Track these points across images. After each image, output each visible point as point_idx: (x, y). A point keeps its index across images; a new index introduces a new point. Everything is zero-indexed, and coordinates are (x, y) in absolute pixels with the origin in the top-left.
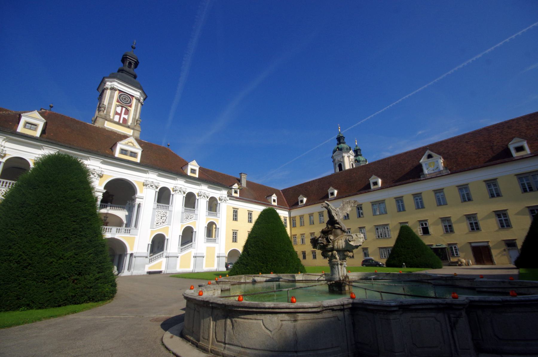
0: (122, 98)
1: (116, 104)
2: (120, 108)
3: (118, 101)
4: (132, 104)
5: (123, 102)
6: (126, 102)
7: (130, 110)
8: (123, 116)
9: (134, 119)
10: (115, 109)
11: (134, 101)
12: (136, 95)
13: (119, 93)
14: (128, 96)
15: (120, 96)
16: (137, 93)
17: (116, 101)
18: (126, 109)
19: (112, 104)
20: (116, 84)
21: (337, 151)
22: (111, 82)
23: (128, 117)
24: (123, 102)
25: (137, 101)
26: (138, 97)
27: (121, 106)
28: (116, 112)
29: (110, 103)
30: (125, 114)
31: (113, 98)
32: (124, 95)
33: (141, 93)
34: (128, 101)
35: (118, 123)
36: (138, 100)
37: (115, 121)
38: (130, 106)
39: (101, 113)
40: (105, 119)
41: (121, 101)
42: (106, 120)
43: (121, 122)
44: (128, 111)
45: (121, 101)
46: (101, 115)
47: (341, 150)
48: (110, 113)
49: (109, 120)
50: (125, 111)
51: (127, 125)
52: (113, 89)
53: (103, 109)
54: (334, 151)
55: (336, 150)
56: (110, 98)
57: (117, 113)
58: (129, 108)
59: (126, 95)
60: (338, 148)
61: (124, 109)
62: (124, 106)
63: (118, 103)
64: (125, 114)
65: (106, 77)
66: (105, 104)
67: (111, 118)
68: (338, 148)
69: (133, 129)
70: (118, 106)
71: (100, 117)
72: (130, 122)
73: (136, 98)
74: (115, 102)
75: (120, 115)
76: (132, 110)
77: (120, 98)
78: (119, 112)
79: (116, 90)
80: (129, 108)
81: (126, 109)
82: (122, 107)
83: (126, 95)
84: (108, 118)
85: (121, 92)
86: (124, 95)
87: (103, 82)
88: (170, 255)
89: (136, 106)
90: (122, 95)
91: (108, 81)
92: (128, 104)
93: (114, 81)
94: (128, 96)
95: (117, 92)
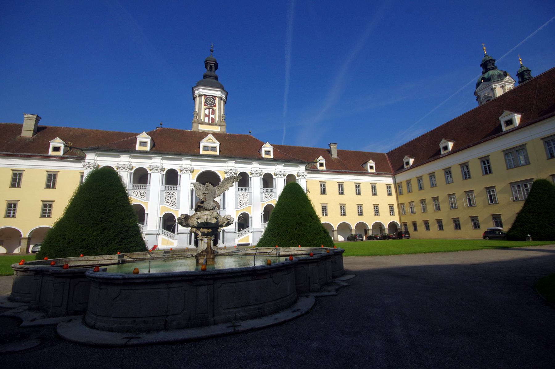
0: (208, 101)
1: (204, 108)
2: (208, 110)
3: (205, 105)
4: (215, 104)
5: (209, 105)
6: (211, 103)
7: (215, 109)
8: (211, 116)
9: (219, 116)
10: (204, 112)
11: (217, 100)
12: (218, 94)
13: (205, 97)
14: (212, 98)
15: (206, 100)
16: (218, 93)
17: (204, 105)
18: (212, 109)
20: (201, 91)
21: (482, 84)
22: (198, 90)
23: (215, 116)
24: (209, 105)
25: (220, 100)
26: (220, 95)
28: (205, 114)
29: (200, 109)
32: (209, 97)
33: (221, 91)
34: (212, 103)
35: (208, 124)
36: (220, 98)
38: (215, 106)
39: (195, 119)
41: (207, 104)
42: (199, 124)
43: (210, 122)
44: (214, 110)
45: (207, 104)
46: (195, 121)
47: (488, 80)
48: (201, 117)
50: (212, 111)
52: (200, 96)
53: (195, 115)
54: (478, 85)
55: (481, 82)
57: (206, 116)
59: (210, 97)
60: (483, 78)
61: (211, 110)
62: (210, 107)
63: (205, 107)
64: (212, 114)
65: (194, 87)
66: (197, 111)
67: (203, 120)
68: (483, 78)
69: (220, 125)
70: (206, 109)
71: (194, 123)
73: (218, 98)
74: (203, 107)
75: (208, 116)
76: (217, 109)
77: (206, 101)
78: (207, 113)
79: (203, 96)
81: (212, 109)
82: (209, 109)
83: (210, 97)
84: (200, 121)
86: (209, 97)
87: (193, 93)
88: (255, 230)
89: (220, 104)
90: (207, 98)
91: (196, 90)
92: (213, 104)
93: (199, 88)
94: (212, 98)
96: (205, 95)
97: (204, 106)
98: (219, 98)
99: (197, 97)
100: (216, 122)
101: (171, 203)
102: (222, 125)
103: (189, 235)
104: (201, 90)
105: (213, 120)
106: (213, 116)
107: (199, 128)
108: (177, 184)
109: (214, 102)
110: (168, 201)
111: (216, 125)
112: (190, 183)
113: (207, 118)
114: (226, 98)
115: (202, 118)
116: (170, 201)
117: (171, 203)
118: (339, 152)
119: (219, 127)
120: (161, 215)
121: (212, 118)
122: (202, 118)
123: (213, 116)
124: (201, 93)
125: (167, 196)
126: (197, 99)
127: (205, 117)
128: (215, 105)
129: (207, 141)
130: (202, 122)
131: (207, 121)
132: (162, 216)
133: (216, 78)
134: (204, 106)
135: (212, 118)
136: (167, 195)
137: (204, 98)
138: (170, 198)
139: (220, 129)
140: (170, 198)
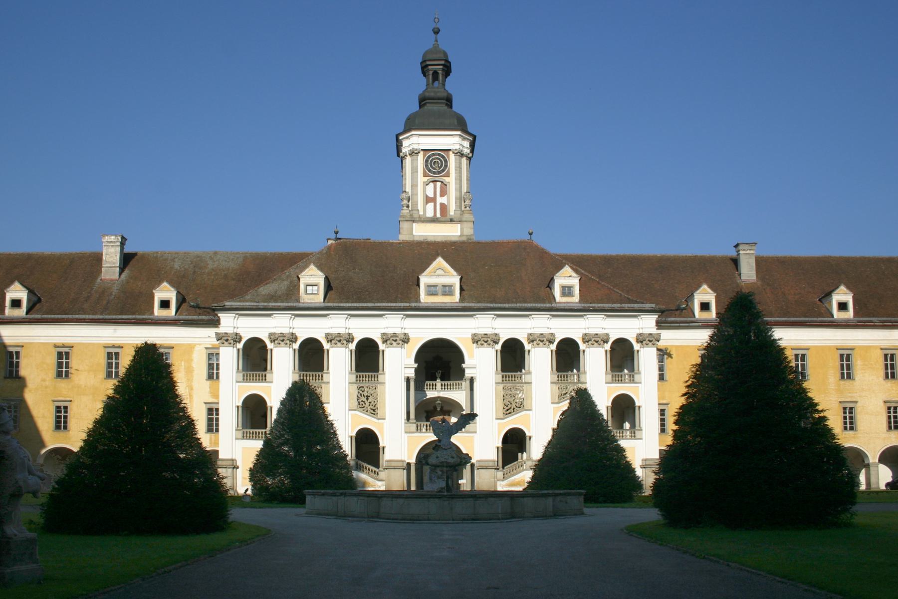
1: (424, 182)
2: (432, 185)
3: (425, 175)
5: (434, 173)
7: (449, 182)
8: (440, 200)
9: (460, 199)
10: (424, 190)
11: (452, 159)
13: (424, 156)
19: (417, 186)
23: (448, 200)
26: (457, 147)
27: (432, 182)
28: (427, 196)
29: (414, 186)
30: (442, 195)
31: (417, 172)
32: (433, 155)
35: (434, 220)
36: (460, 154)
37: (429, 217)
38: (448, 175)
39: (404, 211)
40: (411, 221)
43: (438, 215)
45: (430, 171)
49: (418, 220)
50: (441, 188)
51: (448, 216)
52: (414, 153)
53: (405, 202)
56: (411, 173)
57: (428, 200)
58: (446, 179)
61: (439, 184)
62: (437, 179)
63: (426, 179)
64: (442, 195)
67: (421, 213)
71: (403, 221)
72: (452, 210)
73: (453, 153)
74: (421, 179)
75: (433, 200)
76: (451, 180)
77: (426, 165)
78: (431, 195)
79: (419, 152)
80: (446, 179)
81: (442, 182)
84: (415, 216)
85: (427, 152)
89: (459, 168)
92: (443, 171)
94: (439, 155)
95: (421, 155)
96: (422, 150)
97: (424, 176)
98: (457, 153)
99: (406, 156)
100: (452, 213)
101: (369, 410)
102: (464, 219)
103: (405, 471)
104: (414, 140)
105: (444, 208)
106: (444, 200)
107: (414, 233)
108: (377, 371)
109: (446, 166)
110: (364, 405)
111: (451, 221)
112: (403, 367)
113: (430, 206)
114: (472, 151)
115: (420, 207)
116: (367, 404)
117: (369, 408)
118: (761, 263)
119: (459, 225)
120: (352, 430)
121: (442, 205)
122: (419, 209)
123: (444, 200)
124: (416, 147)
125: (361, 395)
126: (408, 161)
127: (427, 203)
128: (448, 173)
129: (433, 274)
130: (420, 217)
131: (430, 214)
132: (354, 434)
133: (449, 101)
134: (424, 176)
135: (442, 205)
136: (361, 392)
137: (422, 155)
138: (367, 399)
139: (462, 229)
140: (367, 399)
